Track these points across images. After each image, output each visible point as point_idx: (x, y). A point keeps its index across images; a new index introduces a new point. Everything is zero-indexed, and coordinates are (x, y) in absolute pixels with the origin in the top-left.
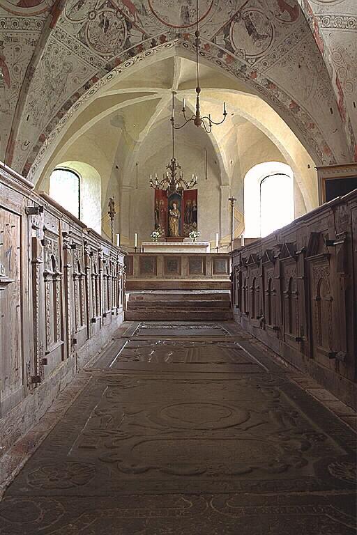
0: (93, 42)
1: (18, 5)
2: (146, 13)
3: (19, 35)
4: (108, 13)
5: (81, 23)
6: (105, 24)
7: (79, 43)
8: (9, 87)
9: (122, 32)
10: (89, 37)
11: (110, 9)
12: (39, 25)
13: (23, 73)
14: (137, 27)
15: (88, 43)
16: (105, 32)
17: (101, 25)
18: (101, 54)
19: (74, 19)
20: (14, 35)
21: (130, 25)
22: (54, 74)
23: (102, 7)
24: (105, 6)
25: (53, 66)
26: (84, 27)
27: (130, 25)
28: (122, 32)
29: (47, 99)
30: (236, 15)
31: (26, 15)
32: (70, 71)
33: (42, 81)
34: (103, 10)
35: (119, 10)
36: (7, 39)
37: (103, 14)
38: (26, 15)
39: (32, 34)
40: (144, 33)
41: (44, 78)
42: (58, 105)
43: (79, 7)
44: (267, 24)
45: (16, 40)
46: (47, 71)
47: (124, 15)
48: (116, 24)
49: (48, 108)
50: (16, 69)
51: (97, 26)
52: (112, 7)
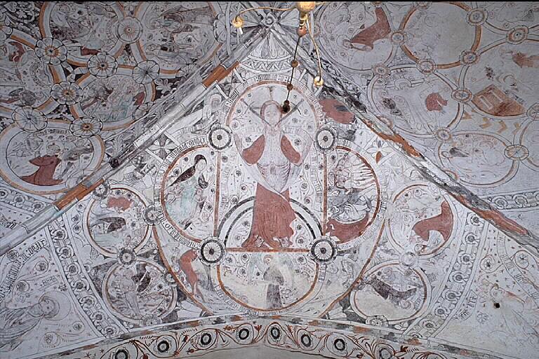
0: (114, 294)
2: (212, 287)
4: (153, 268)
5: (105, 257)
6: (143, 281)
9: (168, 301)
10: (109, 284)
11: (157, 265)
14: (193, 300)
16: (139, 291)
17: (136, 278)
18: (120, 317)
21: (182, 295)
23: (146, 255)
24: (152, 257)
25: (21, 286)
26: (107, 266)
27: (182, 295)
28: (168, 301)
30: (356, 282)
31: (26, 191)
32: (49, 316)
34: (146, 260)
35: (170, 272)
37: (144, 266)
38: (26, 191)
40: (204, 309)
43: (112, 228)
44: (408, 274)
47: (177, 281)
48: (160, 287)
51: (129, 276)
52: (162, 262)
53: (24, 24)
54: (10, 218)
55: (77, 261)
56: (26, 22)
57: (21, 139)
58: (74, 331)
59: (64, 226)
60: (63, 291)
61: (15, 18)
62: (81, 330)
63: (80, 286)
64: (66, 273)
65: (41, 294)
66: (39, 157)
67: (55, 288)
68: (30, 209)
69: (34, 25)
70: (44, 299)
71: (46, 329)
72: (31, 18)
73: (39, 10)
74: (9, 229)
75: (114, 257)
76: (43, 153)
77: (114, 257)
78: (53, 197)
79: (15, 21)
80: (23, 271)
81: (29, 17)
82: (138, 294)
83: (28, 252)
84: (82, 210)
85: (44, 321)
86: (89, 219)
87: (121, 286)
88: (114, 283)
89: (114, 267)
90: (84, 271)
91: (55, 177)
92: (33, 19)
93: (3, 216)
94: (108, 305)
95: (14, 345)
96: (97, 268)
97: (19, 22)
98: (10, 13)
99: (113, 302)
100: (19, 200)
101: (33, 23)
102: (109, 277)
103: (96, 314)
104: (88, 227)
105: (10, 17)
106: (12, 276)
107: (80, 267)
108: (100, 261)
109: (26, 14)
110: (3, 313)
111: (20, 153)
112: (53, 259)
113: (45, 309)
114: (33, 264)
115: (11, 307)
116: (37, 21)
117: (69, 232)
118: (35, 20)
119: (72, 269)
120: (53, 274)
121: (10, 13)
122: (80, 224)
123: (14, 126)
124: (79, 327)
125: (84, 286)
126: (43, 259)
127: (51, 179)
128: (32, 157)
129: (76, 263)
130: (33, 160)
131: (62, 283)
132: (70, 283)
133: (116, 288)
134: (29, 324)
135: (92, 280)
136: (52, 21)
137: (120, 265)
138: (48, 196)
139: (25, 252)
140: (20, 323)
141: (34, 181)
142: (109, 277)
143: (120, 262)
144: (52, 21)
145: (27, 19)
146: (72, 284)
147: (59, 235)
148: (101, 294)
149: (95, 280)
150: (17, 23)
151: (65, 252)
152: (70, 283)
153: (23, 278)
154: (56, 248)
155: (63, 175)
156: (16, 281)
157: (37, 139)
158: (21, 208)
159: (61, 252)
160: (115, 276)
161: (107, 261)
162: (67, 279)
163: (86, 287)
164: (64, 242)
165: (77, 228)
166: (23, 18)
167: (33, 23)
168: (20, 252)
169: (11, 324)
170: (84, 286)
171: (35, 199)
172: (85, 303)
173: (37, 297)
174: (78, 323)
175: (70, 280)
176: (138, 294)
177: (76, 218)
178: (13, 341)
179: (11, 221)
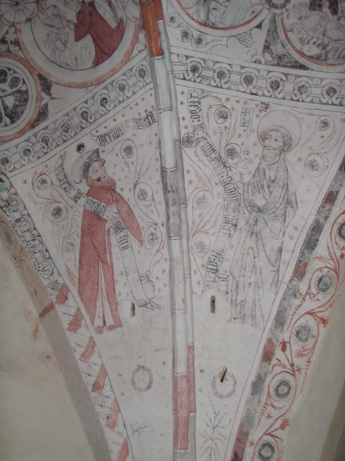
0: (315, 51)
1: (97, 63)
3: (120, 119)
5: (259, 26)
7: (278, 72)
8: (141, 242)
10: (298, 46)
12: (142, 73)
13: (160, 197)
15: (302, 61)
19: (228, 22)
20: (111, 125)
22: (243, 170)
25: (231, 153)
26: (273, 32)
29: (251, 242)
31: (114, 71)
32: (287, 146)
33: (217, 197)
36: (103, 139)
39: (140, 101)
41: (220, 189)
42: (289, 245)
45: (117, 134)
46: (221, 169)
49: (262, 262)
50: (143, 195)
51: (305, 11)
54: (139, 114)
55: (242, 67)
57: (41, 32)
58: (327, 133)
59: (187, 57)
60: (268, 110)
62: (331, 123)
63: (275, 85)
64: (248, 91)
65: (254, 138)
66: (76, 26)
67: (258, 116)
68: (141, 84)
70: (263, 137)
71: (299, 159)
74: (154, 126)
75: (266, 15)
76: (72, 16)
77: (266, 15)
78: (139, 46)
80: (214, 140)
82: (339, 19)
83: (196, 120)
84: (178, 20)
85: (291, 157)
86: (195, 17)
87: (311, 33)
88: (301, 40)
89: (279, 24)
90: (259, 66)
91: (113, 24)
93: (134, 119)
94: (324, 68)
95: (294, 203)
96: (267, 48)
99: (325, 60)
100: (122, 88)
102: (288, 39)
103: (324, 93)
104: (205, 25)
106: (213, 156)
107: (251, 70)
108: (260, 38)
110: (250, 191)
111: (59, 44)
112: (220, 96)
113: (275, 145)
114: (213, 124)
115: (247, 178)
117: (198, 54)
119: (248, 80)
120: (239, 107)
122: (196, 34)
123: (20, 31)
124: (325, 124)
125: (279, 80)
126: (213, 109)
127: (112, 30)
128: (72, 34)
129: (243, 71)
130: (76, 35)
131: (257, 105)
132: (264, 95)
133: (308, 43)
134: (281, 174)
135: (278, 65)
137: (282, 13)
138: (135, 52)
139: (194, 124)
140: (273, 181)
141: (105, 53)
142: (288, 39)
143: (278, 11)
146: (266, 93)
147: (194, 69)
148: (302, 67)
149: (280, 60)
151: (221, 75)
152: (264, 95)
153: (223, 144)
154: (210, 85)
155: (115, 14)
156: (223, 155)
157: (50, 12)
158: (134, 93)
159: (217, 80)
160: (292, 30)
161: (266, 26)
162: (256, 94)
163: (282, 80)
164: (208, 69)
165: (199, 41)
168: (190, 130)
169: (267, 190)
170: (279, 80)
171: (131, 70)
172: (301, 94)
173: (255, 144)
174: (319, 121)
175: (260, 93)
176: (339, 19)
177: (185, 35)
178: (288, 202)
179: (144, 115)
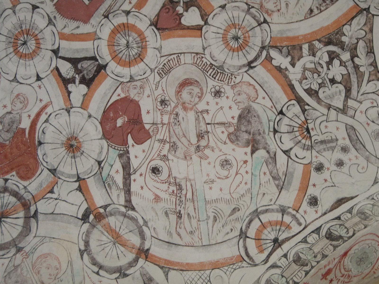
53: (354, 56)
56: (346, 56)
61: (354, 78)
69: (344, 39)
72: (334, 52)
73: (306, 47)
79: (360, 76)
81: (332, 56)
92: (331, 48)
97: (356, 67)
98: (348, 90)
101: (342, 45)
105: (359, 86)
109: (330, 63)
116: (332, 38)
118: (329, 43)
121: (348, 90)
136: (311, 11)
144: (311, 11)
145: (338, 56)
150: (362, 69)
166: (342, 64)
167: (342, 45)
